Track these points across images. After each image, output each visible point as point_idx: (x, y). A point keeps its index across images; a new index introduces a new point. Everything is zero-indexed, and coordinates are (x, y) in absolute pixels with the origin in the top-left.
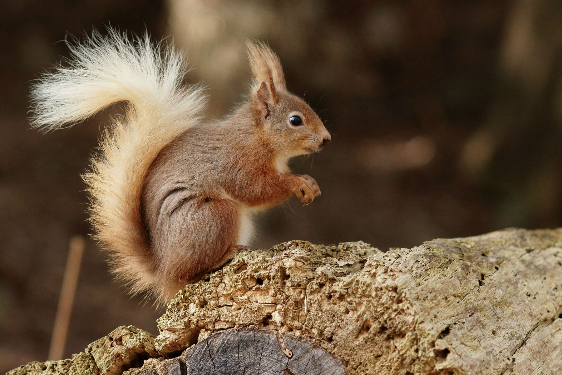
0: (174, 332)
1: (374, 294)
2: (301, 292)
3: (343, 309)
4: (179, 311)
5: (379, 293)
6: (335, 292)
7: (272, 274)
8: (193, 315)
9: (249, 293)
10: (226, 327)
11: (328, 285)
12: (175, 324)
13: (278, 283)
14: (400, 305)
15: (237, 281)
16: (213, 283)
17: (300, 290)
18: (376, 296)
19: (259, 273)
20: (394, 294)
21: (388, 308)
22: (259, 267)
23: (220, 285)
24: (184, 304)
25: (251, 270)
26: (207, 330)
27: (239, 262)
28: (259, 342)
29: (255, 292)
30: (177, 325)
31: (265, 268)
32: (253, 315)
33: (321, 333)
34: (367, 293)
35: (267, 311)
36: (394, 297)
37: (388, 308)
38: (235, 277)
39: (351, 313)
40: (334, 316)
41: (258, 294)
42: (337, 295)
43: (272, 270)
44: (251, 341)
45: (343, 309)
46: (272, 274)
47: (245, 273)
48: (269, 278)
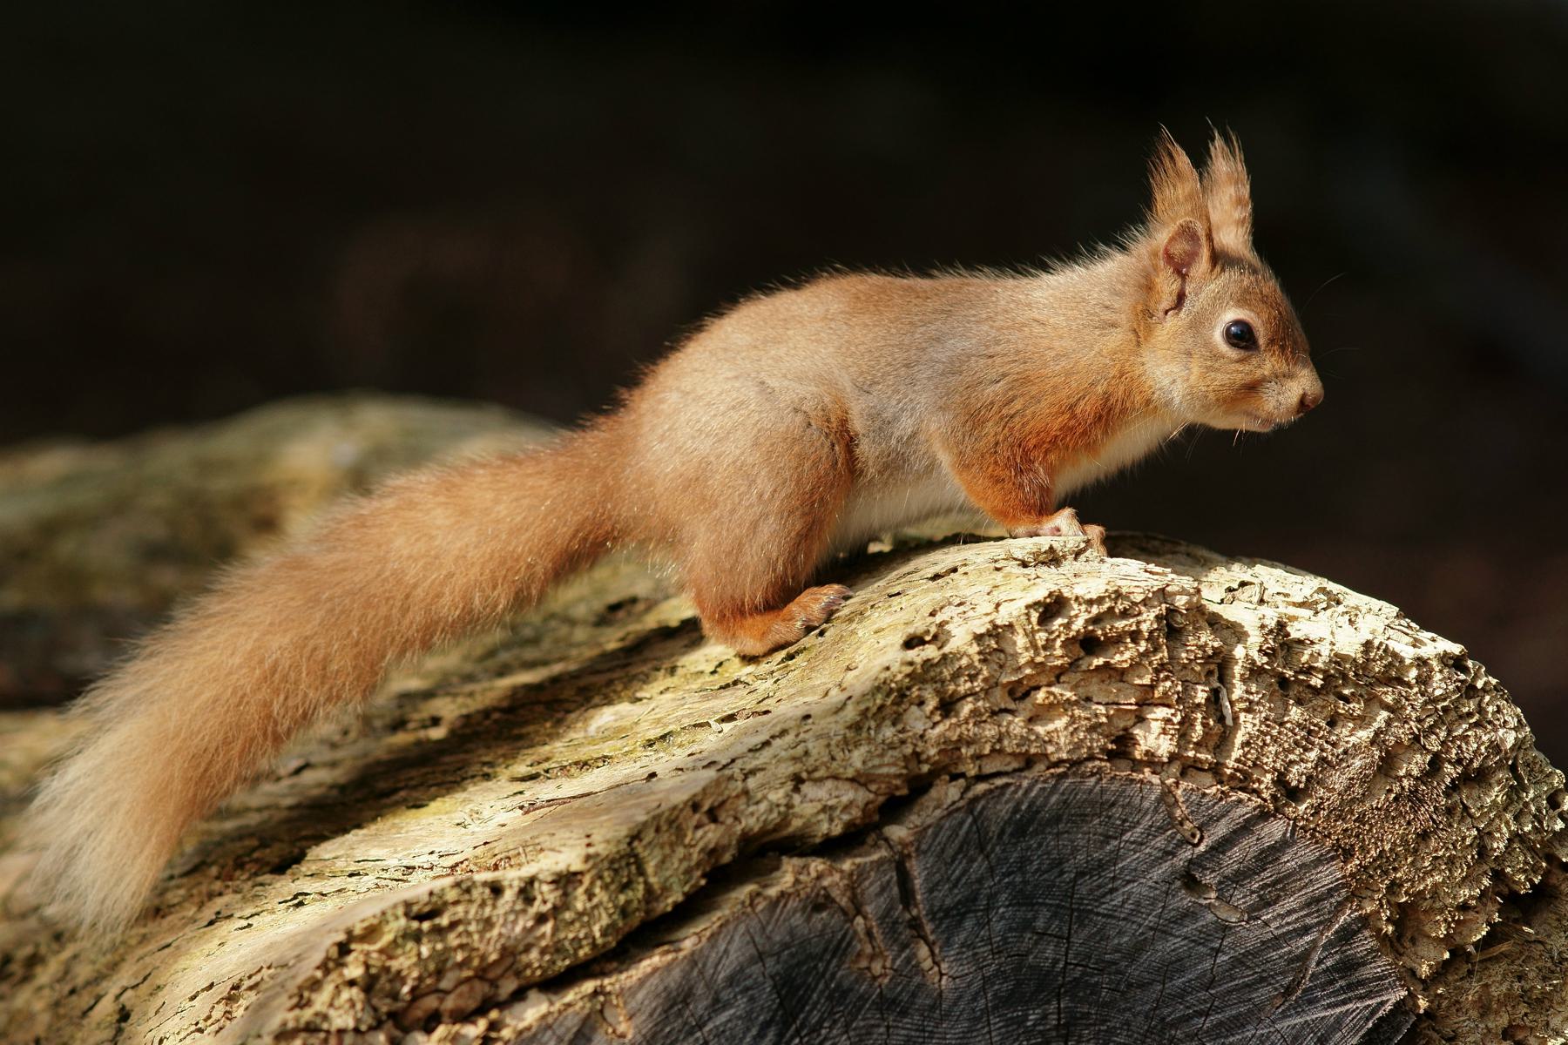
0: (864, 785)
1: (1413, 673)
2: (1210, 673)
4: (878, 727)
8: (922, 736)
9: (1074, 677)
10: (1009, 768)
12: (876, 762)
13: (1156, 649)
15: (1048, 646)
16: (980, 653)
17: (1212, 667)
18: (1418, 678)
22: (1111, 609)
23: (994, 657)
25: (1087, 616)
26: (954, 777)
27: (1050, 595)
28: (1113, 804)
30: (880, 766)
31: (1125, 614)
33: (1281, 781)
35: (1122, 725)
38: (1041, 637)
42: (1317, 681)
43: (1144, 616)
44: (1092, 803)
46: (1144, 627)
47: (1067, 626)
48: (1135, 636)
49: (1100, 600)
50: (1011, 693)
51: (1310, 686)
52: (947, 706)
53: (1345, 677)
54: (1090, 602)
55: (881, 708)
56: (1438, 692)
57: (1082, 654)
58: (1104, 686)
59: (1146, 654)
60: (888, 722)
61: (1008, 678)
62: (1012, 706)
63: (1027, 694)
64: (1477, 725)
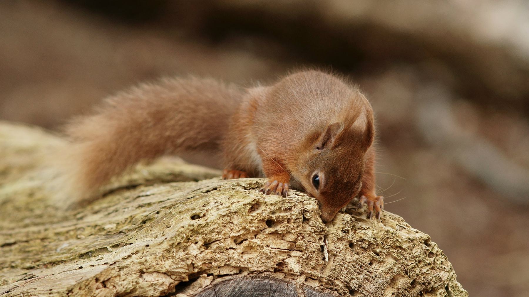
2: (320, 239)
3: (367, 260)
5: (411, 244)
6: (363, 240)
7: (294, 217)
11: (351, 233)
14: (432, 259)
17: (322, 236)
19: (278, 214)
20: (428, 248)
21: (420, 262)
22: (279, 209)
24: (185, 244)
25: (269, 211)
29: (268, 235)
31: (285, 210)
32: (269, 261)
34: (398, 244)
35: (281, 258)
36: (428, 250)
37: (420, 262)
39: (375, 266)
40: (361, 267)
41: (271, 238)
45: (367, 261)
48: (289, 220)
49: (276, 203)
50: (235, 241)
51: (362, 247)
52: (207, 245)
53: (377, 244)
54: (272, 205)
55: (179, 243)
56: (416, 254)
57: (267, 227)
58: (275, 241)
59: (293, 228)
60: (182, 250)
61: (233, 234)
62: (235, 247)
63: (242, 242)
64: (433, 268)
